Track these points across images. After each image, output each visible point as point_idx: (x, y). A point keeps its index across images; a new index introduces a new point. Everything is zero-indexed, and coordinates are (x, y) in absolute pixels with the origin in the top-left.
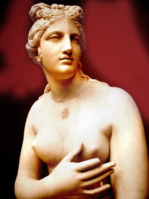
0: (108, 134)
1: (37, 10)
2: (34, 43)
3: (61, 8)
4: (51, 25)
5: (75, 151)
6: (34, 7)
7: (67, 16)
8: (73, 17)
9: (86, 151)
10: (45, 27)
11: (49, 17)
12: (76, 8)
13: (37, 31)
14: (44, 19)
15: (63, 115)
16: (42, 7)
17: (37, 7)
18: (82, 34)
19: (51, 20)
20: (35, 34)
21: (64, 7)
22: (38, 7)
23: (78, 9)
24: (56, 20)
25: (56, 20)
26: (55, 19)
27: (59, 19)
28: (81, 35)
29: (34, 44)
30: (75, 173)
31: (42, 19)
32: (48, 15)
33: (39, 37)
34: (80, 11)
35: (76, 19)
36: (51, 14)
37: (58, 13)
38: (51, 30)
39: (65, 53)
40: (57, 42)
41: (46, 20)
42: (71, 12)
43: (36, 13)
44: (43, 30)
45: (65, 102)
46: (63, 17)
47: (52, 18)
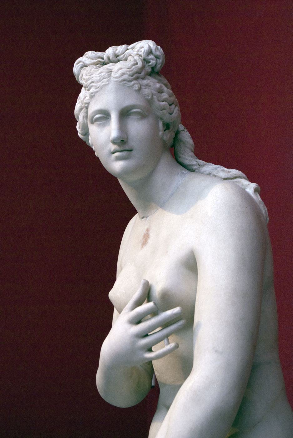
1: (82, 68)
3: (120, 54)
4: (93, 99)
5: (137, 294)
6: (78, 64)
8: (125, 77)
9: (154, 295)
10: (86, 103)
12: (143, 47)
13: (81, 109)
15: (144, 239)
16: (88, 62)
18: (152, 98)
19: (91, 91)
23: (144, 51)
24: (97, 90)
25: (97, 90)
26: (96, 88)
27: (101, 88)
28: (150, 102)
30: (127, 326)
33: (85, 119)
34: (150, 52)
35: (130, 78)
36: (90, 81)
37: (99, 76)
39: (114, 142)
40: (103, 125)
42: (121, 69)
44: (85, 108)
45: (149, 218)
46: (106, 82)
47: (92, 86)
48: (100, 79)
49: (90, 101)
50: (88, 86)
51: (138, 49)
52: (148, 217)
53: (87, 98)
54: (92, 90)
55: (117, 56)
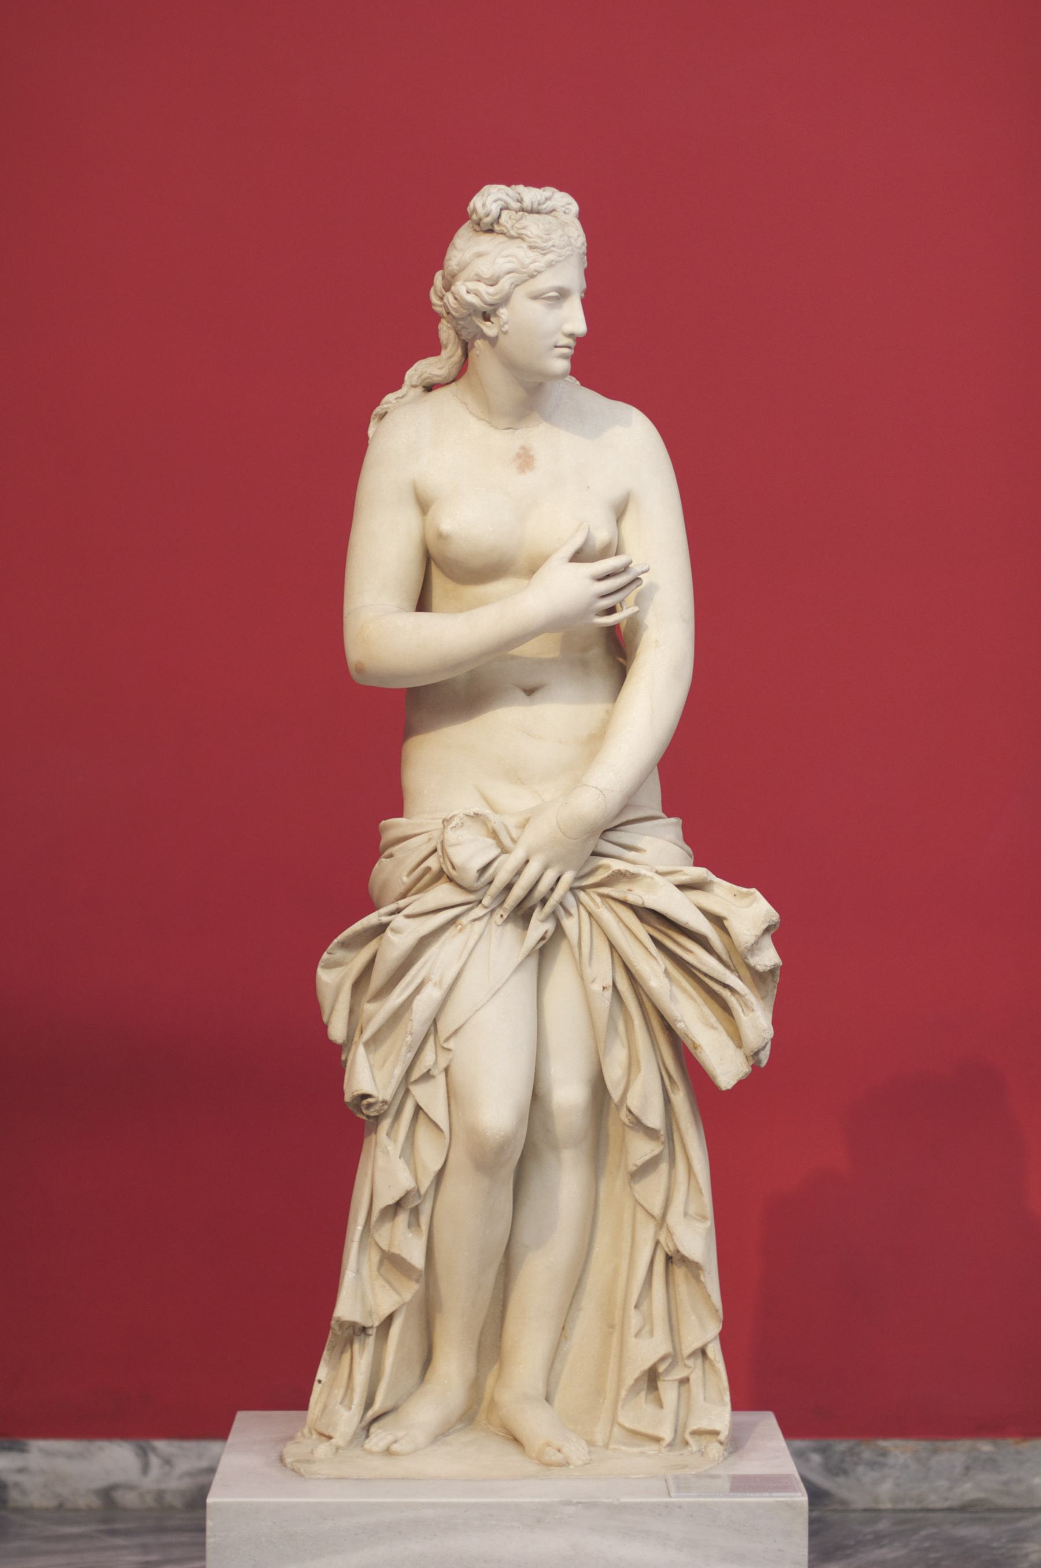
0: (620, 511)
1: (501, 210)
2: (496, 297)
6: (495, 201)
7: (576, 247)
11: (545, 250)
12: (569, 204)
14: (531, 248)
17: (500, 202)
19: (550, 257)
20: (503, 277)
21: (547, 199)
22: (503, 203)
25: (560, 259)
29: (497, 300)
31: (525, 245)
32: (545, 245)
33: (512, 286)
36: (550, 243)
37: (563, 241)
38: (547, 282)
39: (571, 335)
41: (535, 253)
43: (499, 216)
45: (520, 431)
47: (552, 251)
48: (564, 245)
49: (545, 270)
50: (548, 249)
51: (564, 204)
52: (518, 429)
53: (537, 264)
54: (550, 257)
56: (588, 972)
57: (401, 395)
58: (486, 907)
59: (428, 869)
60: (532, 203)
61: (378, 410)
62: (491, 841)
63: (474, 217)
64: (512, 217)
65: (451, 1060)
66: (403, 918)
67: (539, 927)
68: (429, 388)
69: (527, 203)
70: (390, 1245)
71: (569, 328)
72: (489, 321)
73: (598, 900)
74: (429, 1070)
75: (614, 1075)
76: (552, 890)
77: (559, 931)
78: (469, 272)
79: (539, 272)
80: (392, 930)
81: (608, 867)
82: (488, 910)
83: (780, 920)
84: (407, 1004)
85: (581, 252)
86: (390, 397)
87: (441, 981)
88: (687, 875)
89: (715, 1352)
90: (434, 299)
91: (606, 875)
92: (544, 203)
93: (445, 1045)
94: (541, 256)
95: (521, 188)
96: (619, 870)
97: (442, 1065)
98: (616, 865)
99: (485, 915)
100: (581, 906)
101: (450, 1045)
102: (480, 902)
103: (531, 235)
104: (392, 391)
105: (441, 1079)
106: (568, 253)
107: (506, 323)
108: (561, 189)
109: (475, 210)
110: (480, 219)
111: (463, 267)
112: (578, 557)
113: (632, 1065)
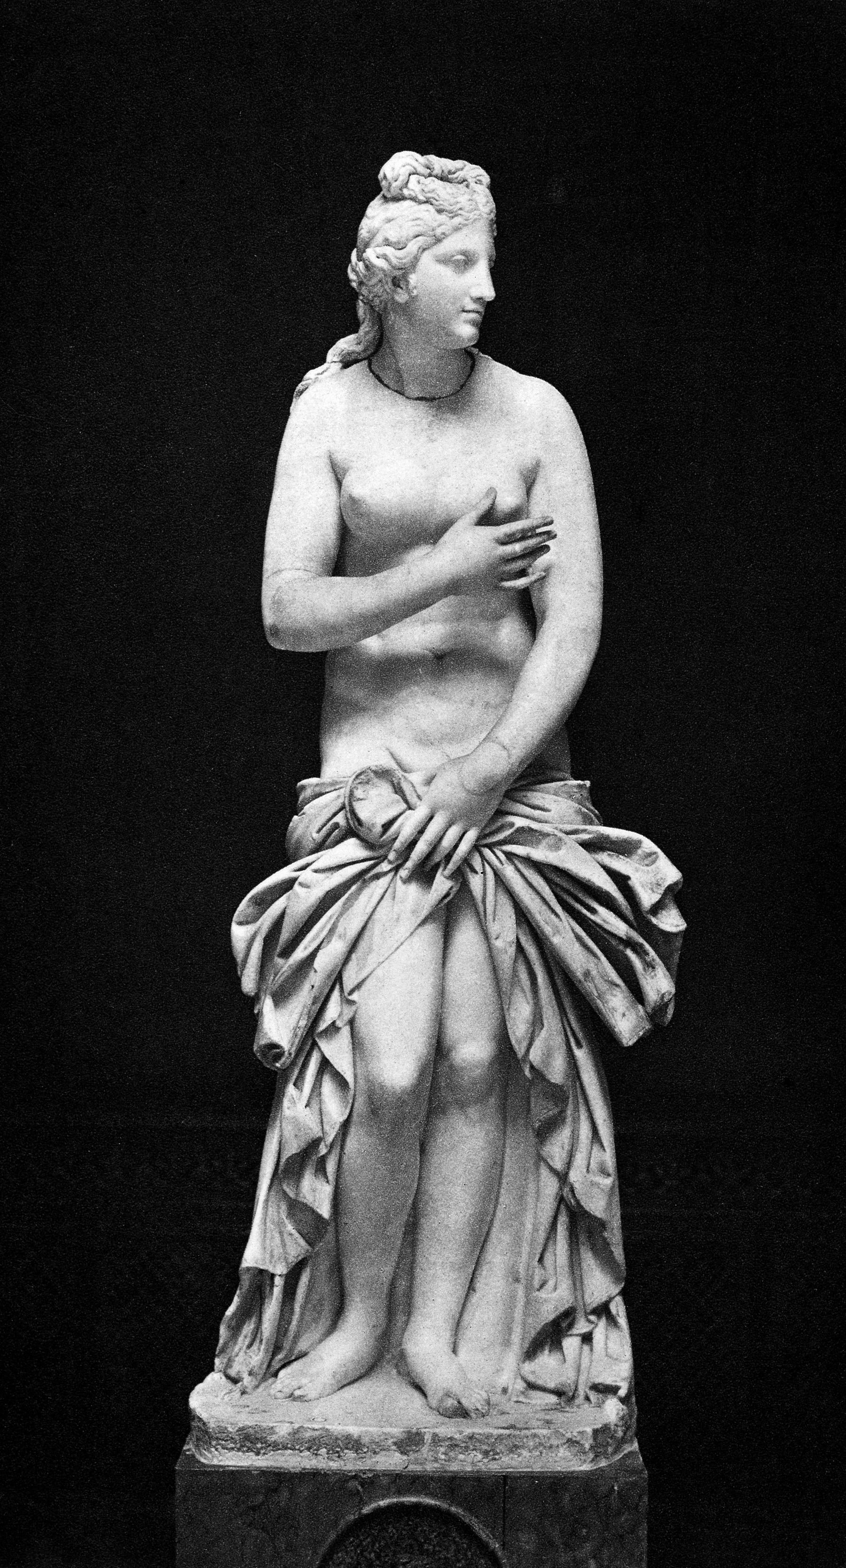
5: (485, 505)
14: (440, 211)
19: (457, 220)
25: (466, 222)
33: (420, 250)
36: (459, 206)
38: (452, 245)
39: (479, 300)
53: (443, 227)
55: (450, 172)
56: (494, 928)
57: (320, 372)
58: (390, 862)
59: (336, 826)
60: (443, 171)
61: (300, 387)
62: (397, 797)
63: (384, 183)
64: (421, 182)
65: (355, 1012)
66: (311, 873)
67: (442, 884)
68: (347, 363)
69: (437, 171)
70: (297, 1194)
71: (476, 293)
72: (399, 286)
73: (502, 857)
74: (334, 1023)
75: (519, 1029)
76: (456, 847)
77: (464, 887)
78: (379, 238)
79: (445, 235)
80: (301, 884)
81: (512, 825)
82: (394, 866)
83: (682, 880)
84: (313, 956)
85: (490, 219)
86: (311, 374)
87: (345, 934)
88: (589, 833)
89: (618, 1308)
90: (352, 276)
91: (511, 831)
92: (454, 173)
93: (350, 998)
94: (448, 219)
95: (433, 158)
96: (523, 828)
97: (347, 1017)
98: (519, 822)
99: (390, 871)
100: (485, 863)
101: (354, 997)
102: (385, 857)
103: (437, 198)
104: (313, 368)
105: (345, 1031)
106: (476, 217)
107: (415, 288)
108: (472, 162)
109: (385, 177)
110: (390, 185)
111: (373, 235)
112: (488, 518)
113: (537, 1021)
